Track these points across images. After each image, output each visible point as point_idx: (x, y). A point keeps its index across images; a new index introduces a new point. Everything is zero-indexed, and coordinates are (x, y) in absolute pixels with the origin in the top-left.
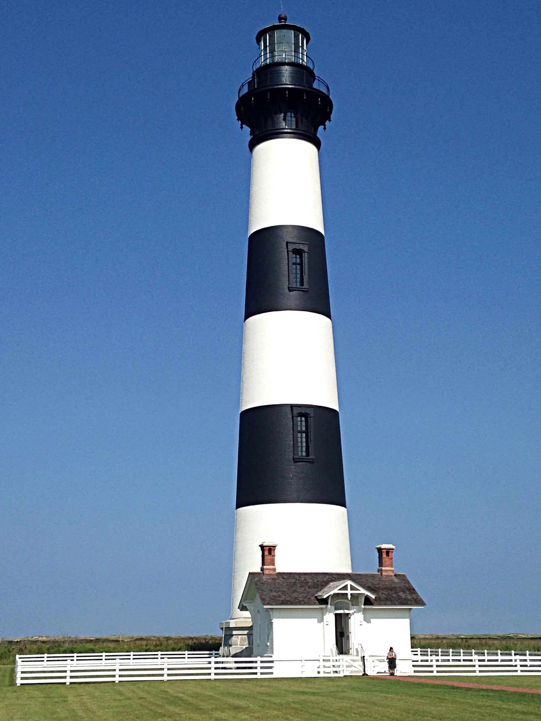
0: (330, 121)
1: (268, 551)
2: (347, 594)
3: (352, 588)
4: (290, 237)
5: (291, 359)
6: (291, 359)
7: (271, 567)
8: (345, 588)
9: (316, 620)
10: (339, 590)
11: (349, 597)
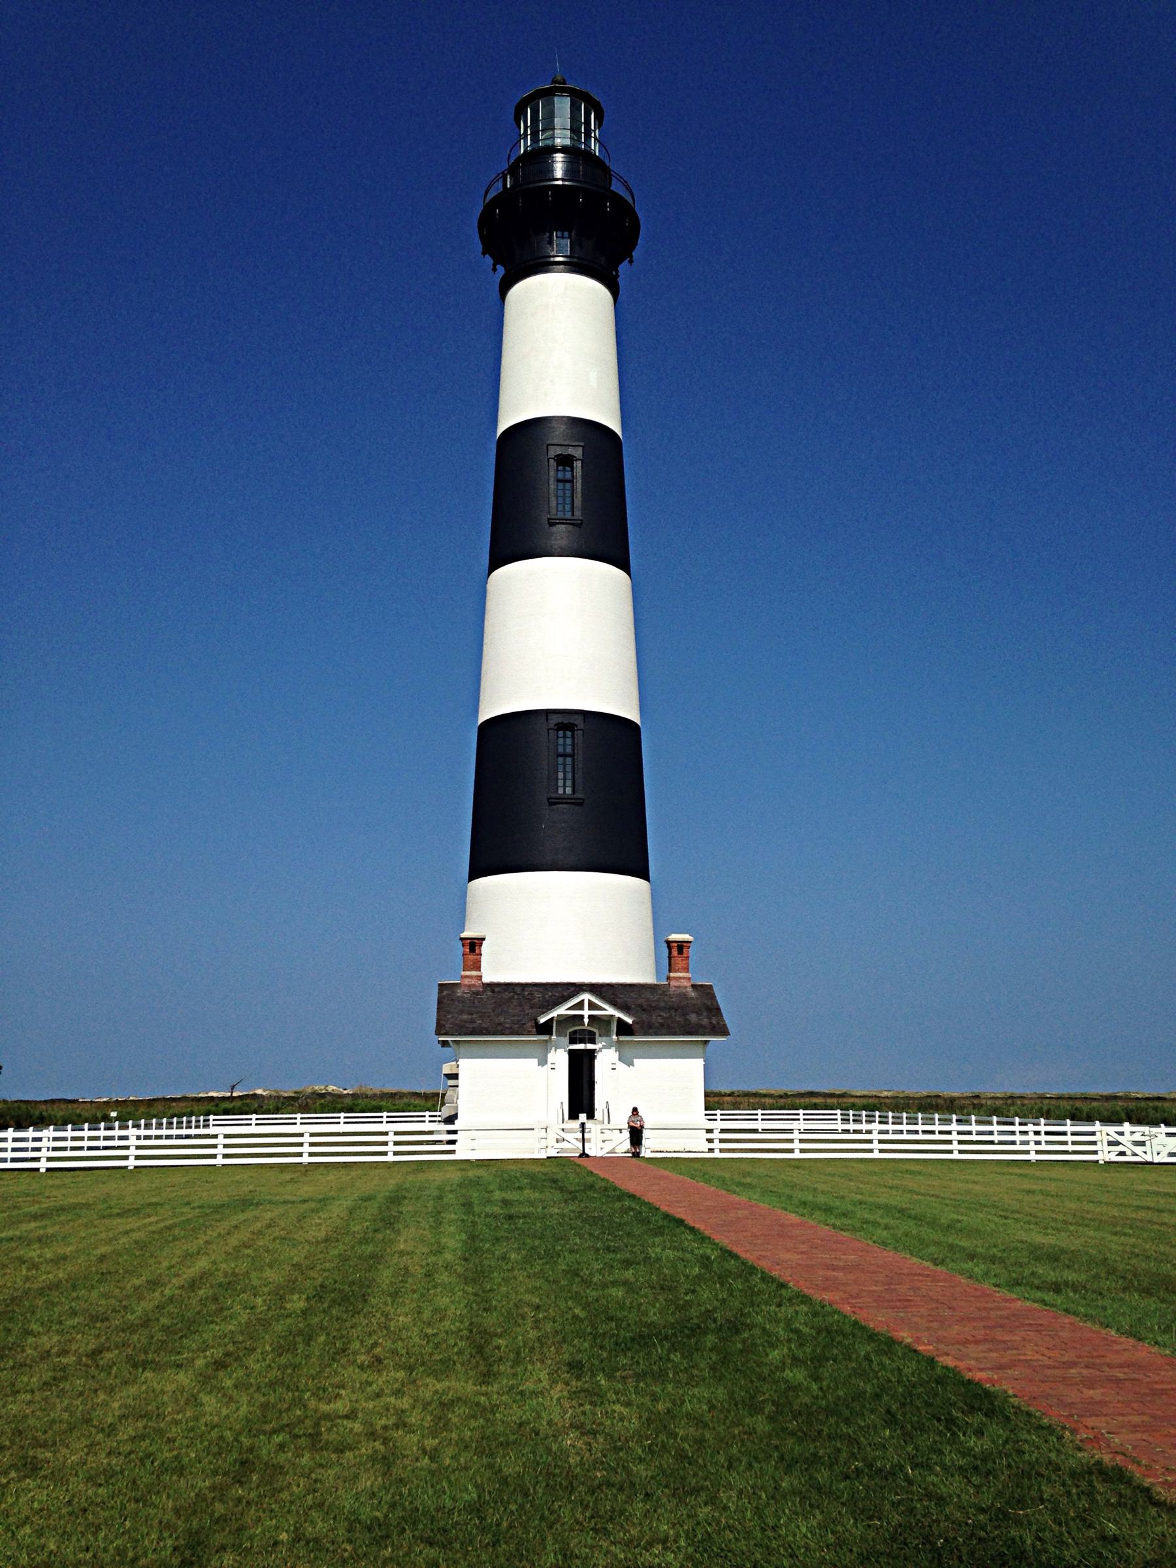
2: (582, 1016)
3: (592, 1006)
4: (558, 434)
5: (559, 636)
6: (559, 636)
7: (474, 973)
8: (580, 1006)
9: (535, 1061)
10: (569, 1009)
11: (586, 1021)
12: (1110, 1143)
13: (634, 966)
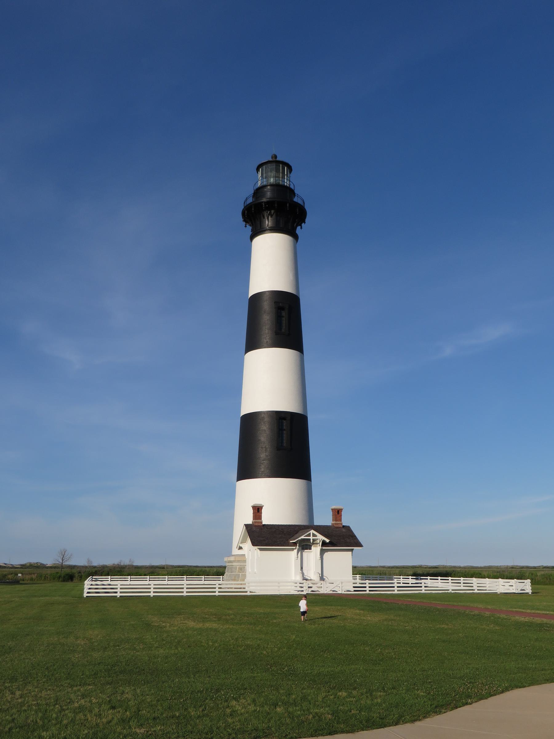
0: (305, 223)
1: (257, 510)
3: (314, 535)
11: (312, 541)
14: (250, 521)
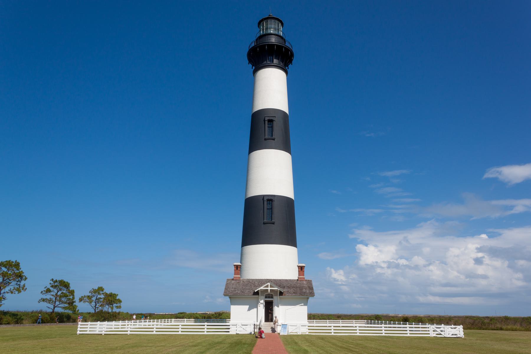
5: (273, 173)
6: (273, 173)
12: (434, 331)
13: (290, 273)
14: (232, 276)
